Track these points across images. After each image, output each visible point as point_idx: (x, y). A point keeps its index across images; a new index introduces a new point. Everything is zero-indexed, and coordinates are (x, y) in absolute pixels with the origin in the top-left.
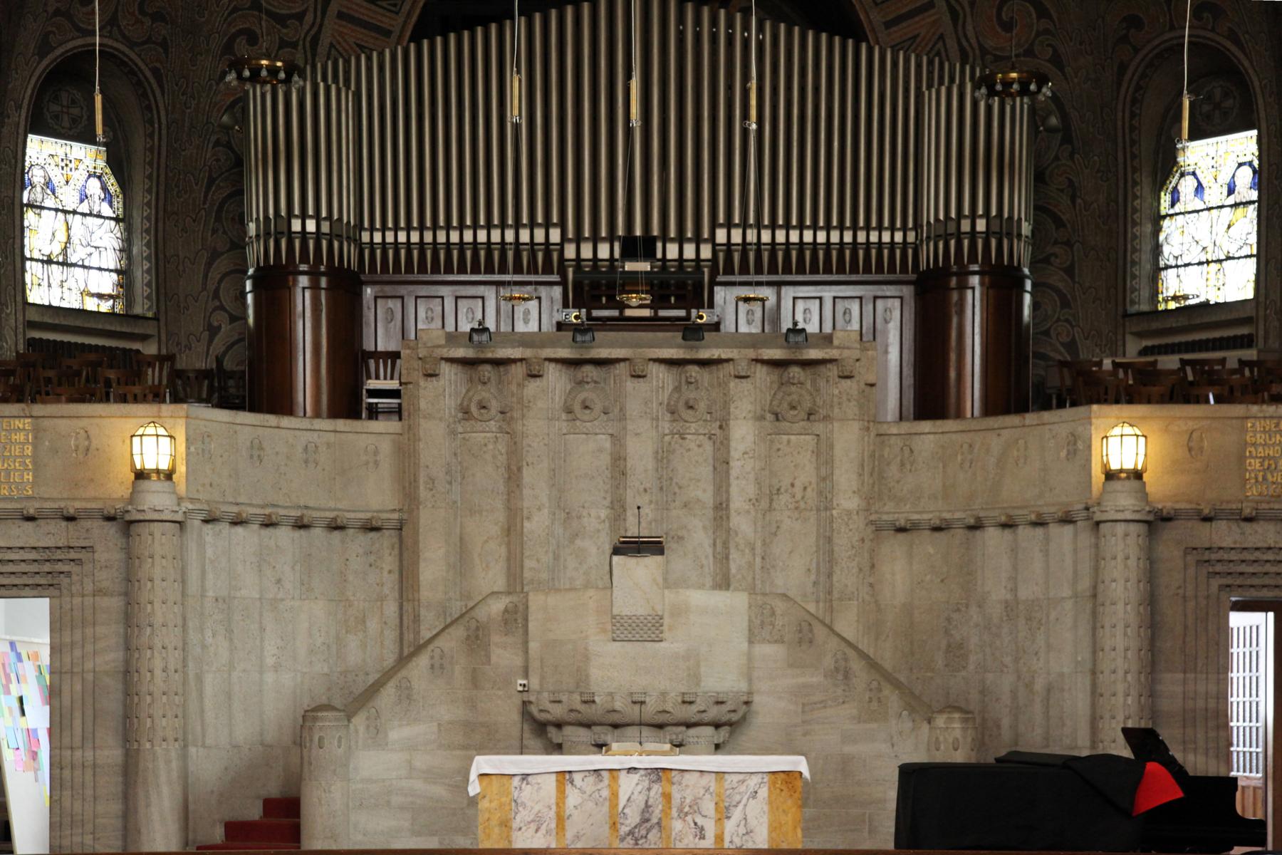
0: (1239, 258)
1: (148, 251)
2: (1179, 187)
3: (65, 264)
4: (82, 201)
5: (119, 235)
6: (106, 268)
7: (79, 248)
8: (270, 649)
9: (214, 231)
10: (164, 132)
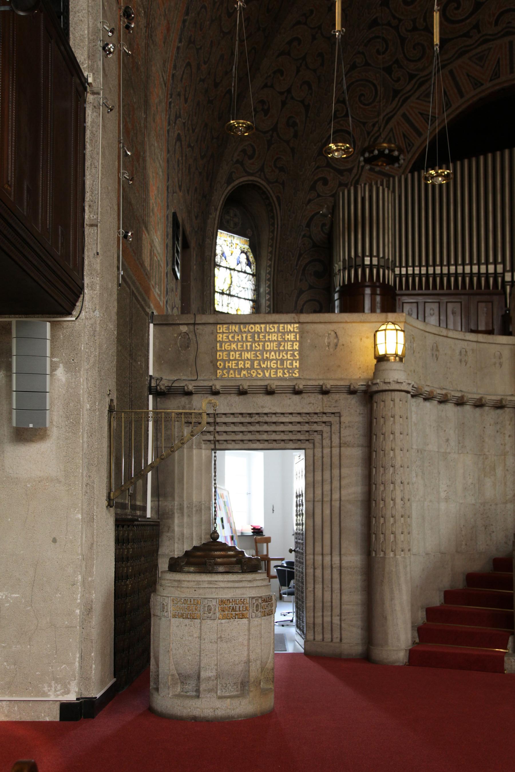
1: (269, 290)
3: (229, 295)
4: (238, 264)
5: (253, 283)
6: (248, 298)
7: (236, 288)
9: (301, 280)
10: (279, 229)
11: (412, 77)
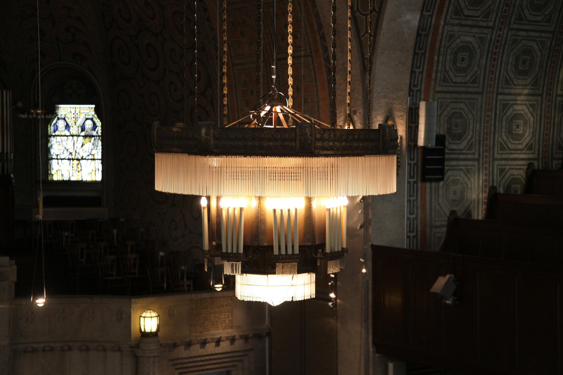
0: (88, 159)
2: (57, 124)
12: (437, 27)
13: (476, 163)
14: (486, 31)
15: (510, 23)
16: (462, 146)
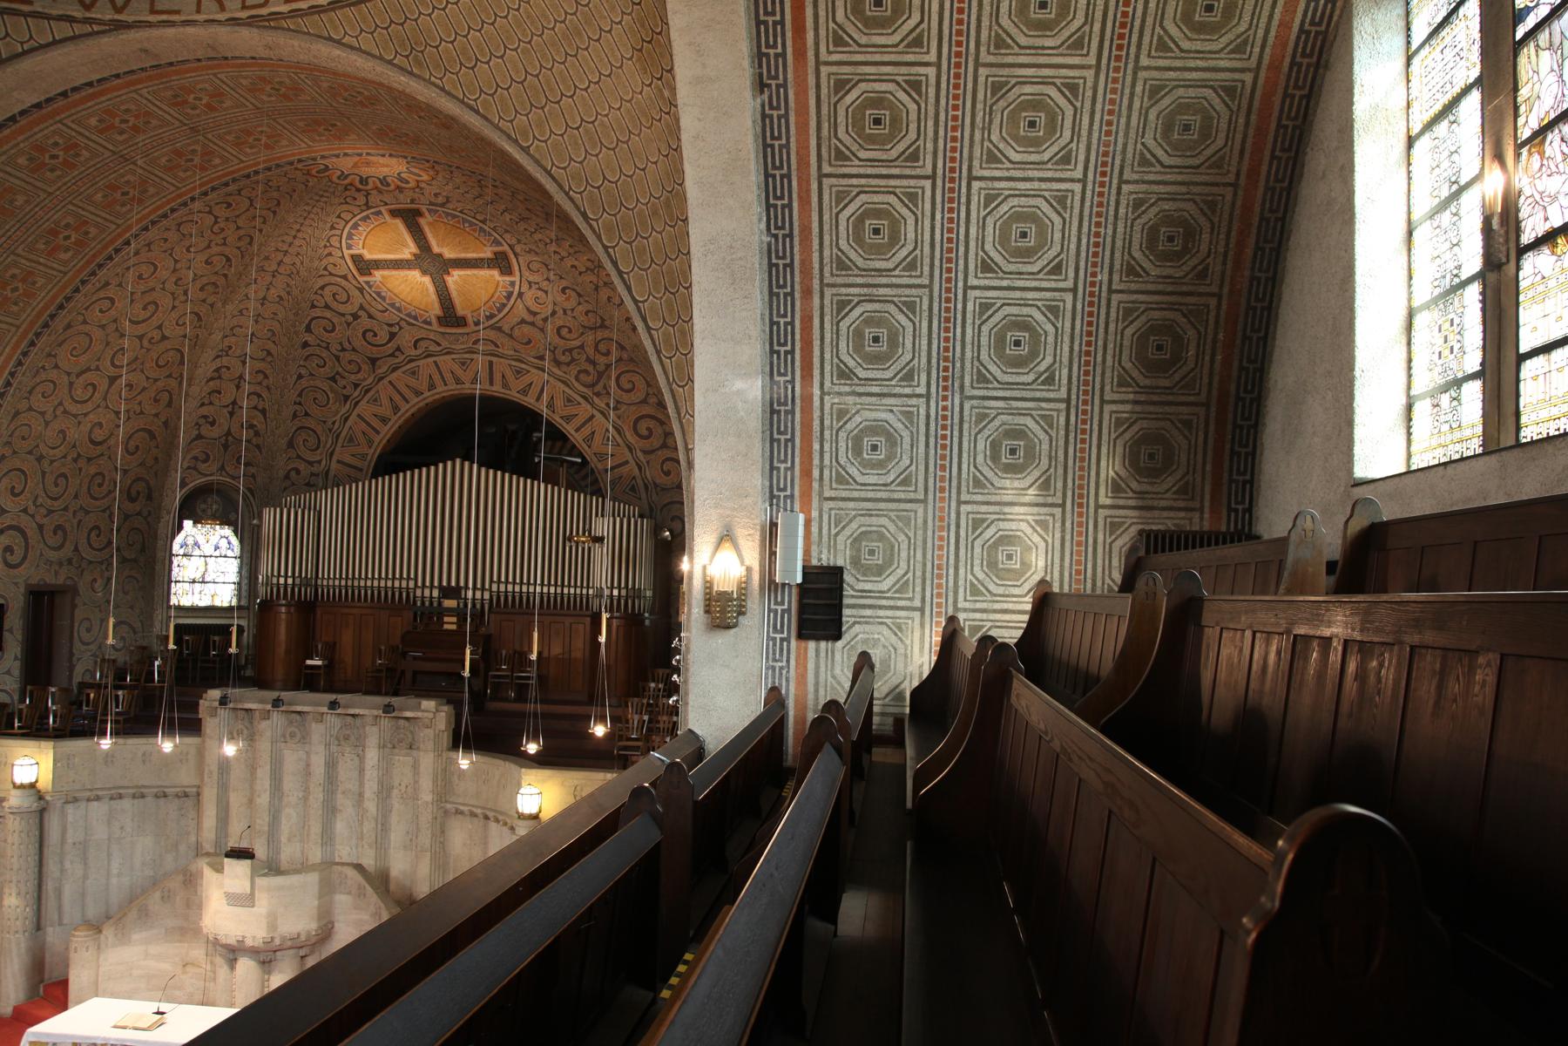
3: (203, 582)
8: (115, 867)
11: (356, 386)
12: (807, 400)
13: (917, 614)
14: (914, 401)
15: (962, 387)
16: (885, 586)
